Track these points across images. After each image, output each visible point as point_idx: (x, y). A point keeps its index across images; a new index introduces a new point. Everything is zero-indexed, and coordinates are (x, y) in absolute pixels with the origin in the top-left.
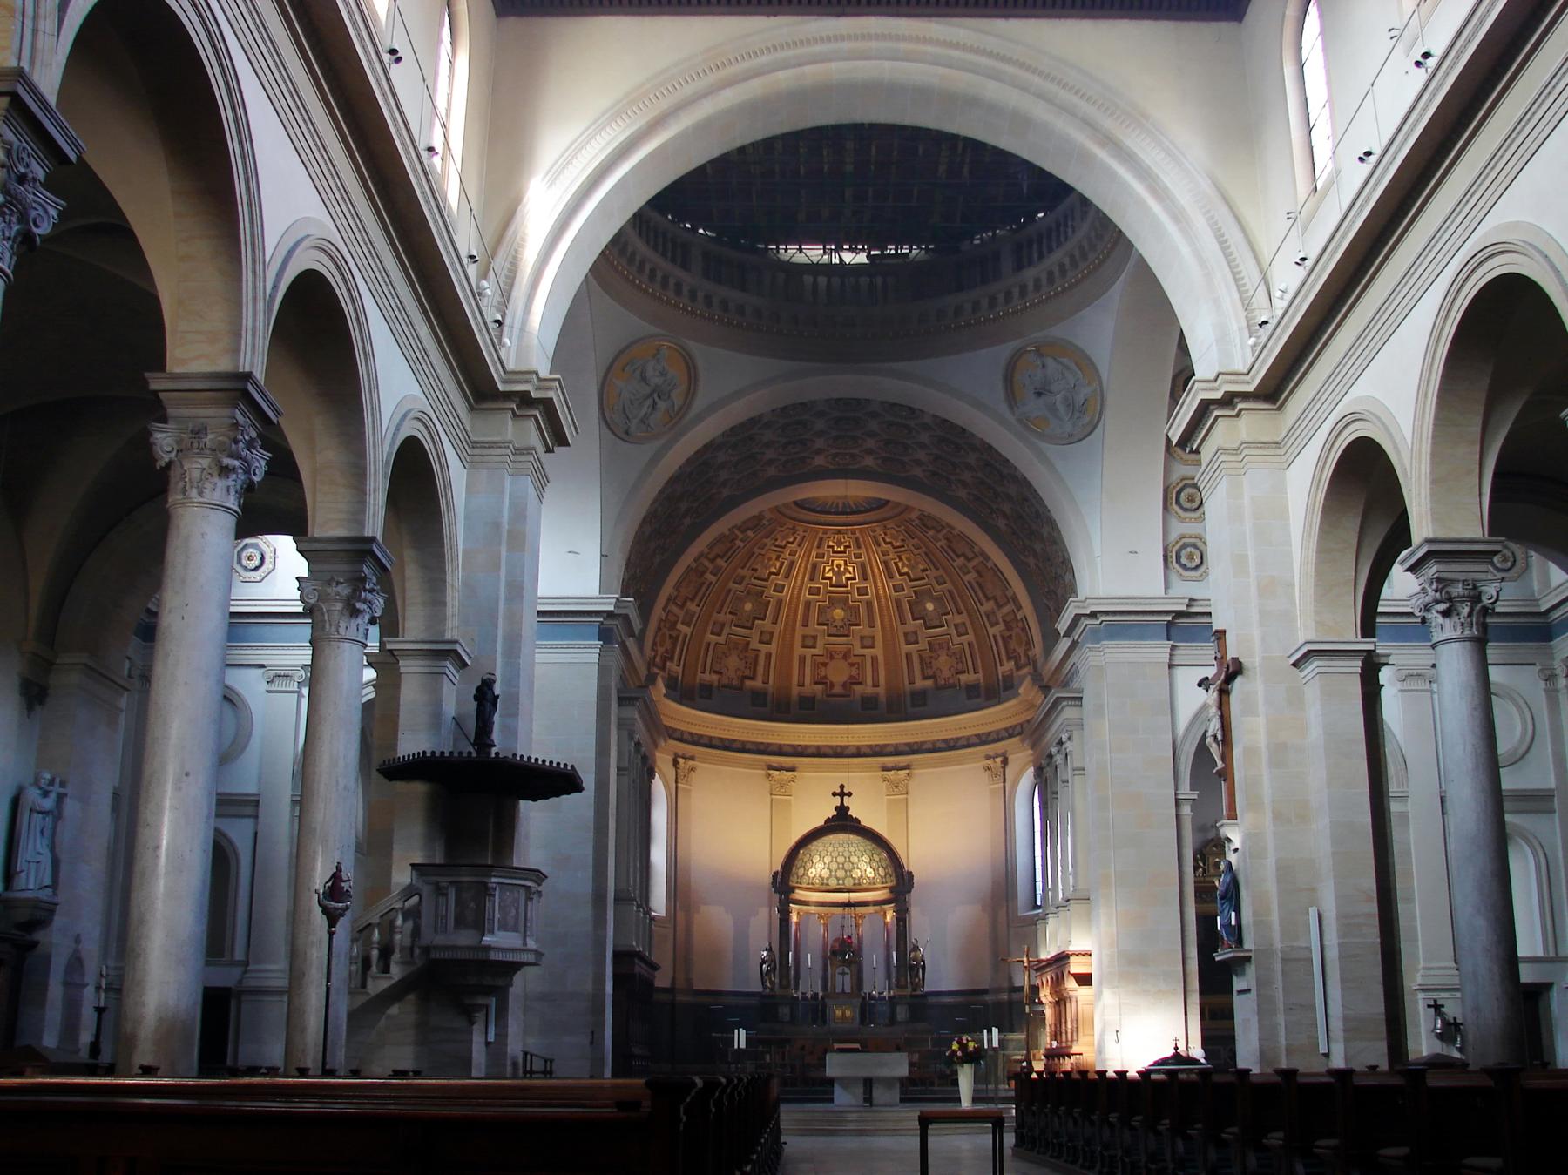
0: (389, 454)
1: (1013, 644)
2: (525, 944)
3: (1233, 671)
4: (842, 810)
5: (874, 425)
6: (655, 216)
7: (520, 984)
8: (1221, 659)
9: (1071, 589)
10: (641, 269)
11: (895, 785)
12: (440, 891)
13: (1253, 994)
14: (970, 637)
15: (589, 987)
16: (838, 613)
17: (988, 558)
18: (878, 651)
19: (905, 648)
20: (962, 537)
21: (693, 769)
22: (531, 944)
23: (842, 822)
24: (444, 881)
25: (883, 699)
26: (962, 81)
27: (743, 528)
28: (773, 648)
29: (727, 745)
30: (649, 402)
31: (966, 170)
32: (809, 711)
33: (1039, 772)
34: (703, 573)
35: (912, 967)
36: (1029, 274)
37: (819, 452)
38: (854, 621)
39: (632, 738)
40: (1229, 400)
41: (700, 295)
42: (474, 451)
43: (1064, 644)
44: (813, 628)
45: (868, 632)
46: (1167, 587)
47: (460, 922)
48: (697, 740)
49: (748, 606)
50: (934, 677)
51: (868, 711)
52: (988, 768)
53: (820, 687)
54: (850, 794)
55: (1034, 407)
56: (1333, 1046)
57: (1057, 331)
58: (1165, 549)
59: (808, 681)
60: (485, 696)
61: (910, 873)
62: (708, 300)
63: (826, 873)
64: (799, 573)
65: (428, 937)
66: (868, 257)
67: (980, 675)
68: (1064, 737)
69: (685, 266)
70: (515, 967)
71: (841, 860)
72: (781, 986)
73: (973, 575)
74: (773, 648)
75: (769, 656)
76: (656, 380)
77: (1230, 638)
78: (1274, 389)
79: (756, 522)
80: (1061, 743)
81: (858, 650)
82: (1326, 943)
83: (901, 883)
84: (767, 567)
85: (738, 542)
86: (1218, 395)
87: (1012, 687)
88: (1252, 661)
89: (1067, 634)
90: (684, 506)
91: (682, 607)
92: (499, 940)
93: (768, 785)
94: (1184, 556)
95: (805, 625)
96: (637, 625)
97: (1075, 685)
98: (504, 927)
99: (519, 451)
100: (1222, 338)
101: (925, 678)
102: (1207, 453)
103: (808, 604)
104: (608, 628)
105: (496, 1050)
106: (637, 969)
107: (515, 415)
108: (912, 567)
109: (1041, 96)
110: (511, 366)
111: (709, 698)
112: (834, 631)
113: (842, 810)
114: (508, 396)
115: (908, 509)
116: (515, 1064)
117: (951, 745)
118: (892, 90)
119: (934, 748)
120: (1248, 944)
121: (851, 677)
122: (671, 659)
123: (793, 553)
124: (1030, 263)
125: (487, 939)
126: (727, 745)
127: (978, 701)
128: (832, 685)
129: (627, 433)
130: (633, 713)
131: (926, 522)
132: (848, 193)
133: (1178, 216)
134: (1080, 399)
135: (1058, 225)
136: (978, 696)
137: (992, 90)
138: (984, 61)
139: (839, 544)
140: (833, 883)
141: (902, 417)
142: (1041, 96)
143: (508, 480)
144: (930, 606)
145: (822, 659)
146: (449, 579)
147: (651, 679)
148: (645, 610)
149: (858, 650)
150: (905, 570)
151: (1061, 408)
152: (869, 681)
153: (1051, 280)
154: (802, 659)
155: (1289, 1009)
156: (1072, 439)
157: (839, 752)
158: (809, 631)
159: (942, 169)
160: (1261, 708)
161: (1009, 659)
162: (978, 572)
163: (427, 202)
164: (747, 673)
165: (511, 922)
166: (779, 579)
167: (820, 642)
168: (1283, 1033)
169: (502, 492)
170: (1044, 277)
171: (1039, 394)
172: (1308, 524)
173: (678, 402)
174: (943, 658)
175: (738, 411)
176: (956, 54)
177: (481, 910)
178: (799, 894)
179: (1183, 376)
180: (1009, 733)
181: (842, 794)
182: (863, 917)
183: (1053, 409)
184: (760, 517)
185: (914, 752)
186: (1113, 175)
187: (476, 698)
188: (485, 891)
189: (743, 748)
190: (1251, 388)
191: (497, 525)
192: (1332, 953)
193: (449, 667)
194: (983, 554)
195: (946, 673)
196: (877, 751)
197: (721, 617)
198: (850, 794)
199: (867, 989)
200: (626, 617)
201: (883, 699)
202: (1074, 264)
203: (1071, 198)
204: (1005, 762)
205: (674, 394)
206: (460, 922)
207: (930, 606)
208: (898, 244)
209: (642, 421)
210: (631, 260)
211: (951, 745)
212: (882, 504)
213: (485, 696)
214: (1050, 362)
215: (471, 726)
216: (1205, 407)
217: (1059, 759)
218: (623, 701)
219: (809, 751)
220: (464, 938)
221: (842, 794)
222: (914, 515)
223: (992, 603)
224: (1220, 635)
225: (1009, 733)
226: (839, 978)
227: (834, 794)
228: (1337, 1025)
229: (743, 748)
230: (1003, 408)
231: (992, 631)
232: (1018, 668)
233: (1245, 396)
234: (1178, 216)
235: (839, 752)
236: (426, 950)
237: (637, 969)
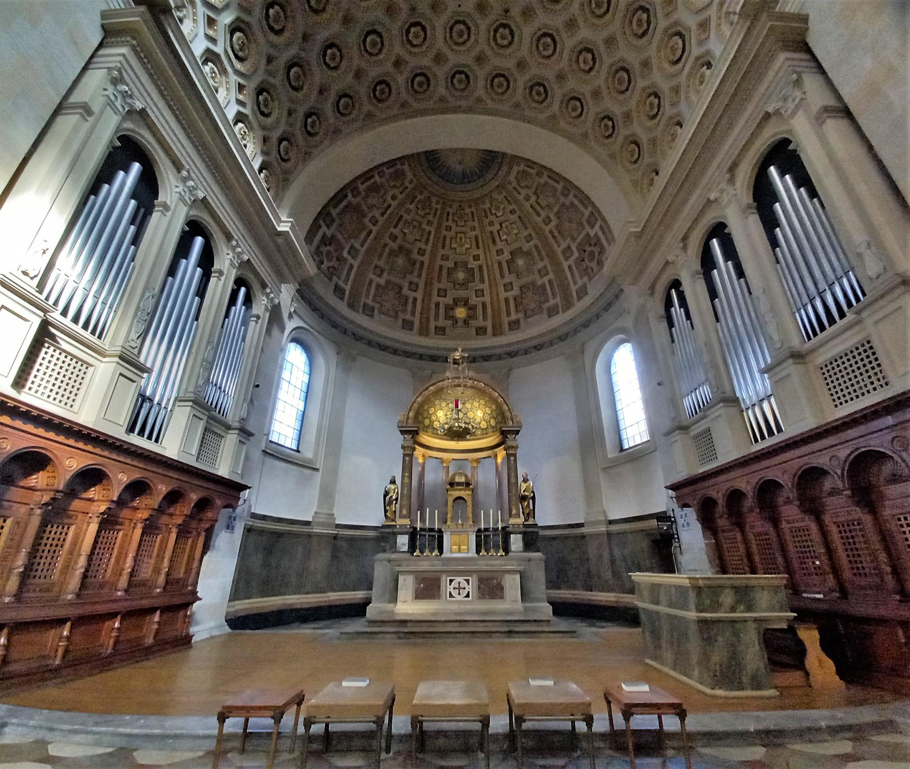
16: (461, 275)
18: (487, 299)
19: (503, 295)
35: (524, 498)
48: (358, 338)
67: (558, 300)
75: (415, 299)
136: (558, 313)
154: (437, 305)
178: (425, 439)
182: (478, 461)
195: (532, 306)
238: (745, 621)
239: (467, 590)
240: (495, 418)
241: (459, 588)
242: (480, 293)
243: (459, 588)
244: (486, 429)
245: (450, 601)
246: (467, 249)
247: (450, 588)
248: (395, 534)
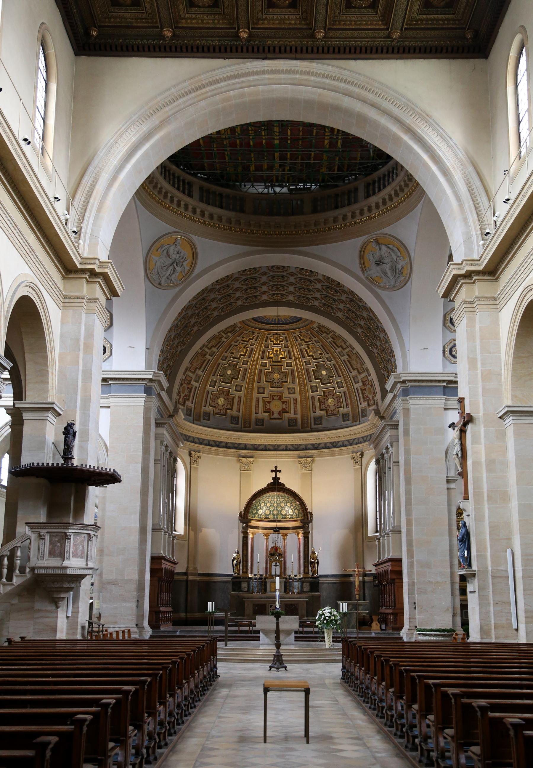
0: (9, 307)
1: (366, 393)
2: (87, 565)
3: (468, 420)
4: (276, 479)
5: (292, 279)
6: (174, 167)
7: (85, 584)
8: (462, 413)
9: (394, 368)
10: (165, 196)
11: (305, 466)
12: (41, 537)
13: (477, 594)
14: (345, 389)
15: (135, 576)
16: (276, 376)
17: (353, 349)
18: (297, 396)
20: (340, 337)
21: (199, 457)
22: (90, 565)
23: (276, 486)
24: (43, 532)
25: (299, 421)
26: (330, 97)
27: (226, 331)
28: (242, 393)
29: (218, 444)
30: (172, 267)
31: (340, 142)
32: (261, 427)
33: (378, 462)
34: (205, 355)
35: (312, 563)
36: (373, 200)
37: (264, 293)
38: (284, 380)
39: (162, 444)
40: (468, 275)
41: (198, 210)
42: (66, 301)
43: (390, 396)
44: (263, 384)
45: (291, 385)
46: (444, 368)
47: (52, 554)
48: (201, 442)
49: (229, 372)
50: (326, 410)
51: (292, 427)
52: (353, 458)
53: (267, 414)
54: (280, 471)
55: (374, 271)
56: (520, 625)
57: (387, 230)
58: (444, 347)
59: (260, 411)
60: (69, 432)
62: (203, 214)
63: (268, 512)
64: (256, 354)
65: (34, 561)
66: (289, 189)
67: (350, 409)
68: (389, 445)
69: (190, 195)
70: (83, 577)
71: (275, 505)
72: (243, 572)
73: (346, 357)
74: (242, 393)
75: (240, 397)
76: (174, 256)
77: (467, 402)
78: (493, 270)
79: (232, 329)
80: (387, 448)
81: (287, 395)
82: (516, 569)
83: (306, 518)
84: (239, 352)
85: (223, 339)
86: (463, 272)
87: (366, 416)
88: (479, 414)
89: (391, 391)
90: (193, 321)
91: (194, 373)
92: (73, 563)
93: (238, 465)
94: (450, 352)
95: (259, 382)
96: (166, 385)
97: (395, 418)
98: (75, 555)
99: (90, 301)
100: (468, 239)
101: (321, 410)
102: (457, 303)
103: (260, 371)
104: (149, 387)
105: (72, 620)
106: (163, 566)
107: (88, 281)
108: (315, 352)
109: (373, 105)
110: (86, 255)
111: (209, 420)
112: (274, 385)
113: (276, 479)
114: (83, 271)
115: (312, 322)
116: (83, 628)
117: (334, 445)
118: (294, 102)
119: (326, 447)
120: (474, 567)
121: (283, 409)
122: (188, 400)
123: (252, 345)
124: (374, 194)
125: (66, 563)
126: (218, 444)
127: (348, 422)
128: (273, 413)
129: (160, 284)
130: (163, 431)
131: (321, 328)
132: (277, 155)
133: (446, 173)
134: (399, 267)
135: (389, 172)
136: (348, 420)
137: (346, 102)
138: (342, 85)
139: (277, 339)
140: (271, 517)
141: (306, 276)
142: (373, 105)
143: (84, 316)
144: (324, 373)
145: (268, 400)
146: (50, 370)
147: (176, 411)
148: (171, 378)
149: (287, 395)
150: (311, 354)
151: (389, 273)
152: (292, 411)
153: (384, 203)
154: (258, 400)
155: (496, 604)
156: (394, 288)
157: (276, 448)
158: (261, 385)
159: (326, 142)
160: (483, 441)
161: (364, 401)
162: (348, 355)
163: (26, 169)
164: (229, 407)
165: (80, 554)
166: (245, 358)
167: (267, 391)
168: (492, 616)
169: (80, 323)
170: (381, 201)
171: (378, 264)
172: (509, 343)
173: (187, 268)
174: (331, 400)
175: (220, 273)
176: (327, 81)
177: (63, 547)
178: (253, 523)
179: (450, 258)
180: (365, 439)
181: (276, 471)
183: (385, 274)
184: (235, 326)
185: (316, 448)
186: (411, 149)
187: (64, 433)
188: (65, 536)
189: (226, 446)
190: (481, 268)
191: (78, 341)
192: (519, 575)
193: (50, 416)
194: (350, 346)
195: (332, 408)
196: (296, 448)
197: (214, 378)
198: (280, 471)
199: (289, 572)
200: (159, 381)
201: (299, 421)
202: (397, 195)
203: (391, 163)
204: (362, 455)
205: (185, 264)
206: (52, 554)
207: (324, 373)
208: (305, 182)
209: (168, 278)
210: (160, 192)
211: (334, 445)
212: (299, 319)
213: (69, 432)
214: (383, 248)
215: (61, 447)
216: (456, 279)
217: (386, 456)
218: (157, 424)
219: (260, 447)
220: (54, 562)
221: (276, 471)
222: (315, 325)
223: (356, 371)
224: (462, 401)
225: (365, 439)
226: (273, 568)
227: (272, 471)
228: (521, 614)
229: (226, 446)
230: (359, 272)
231: (356, 386)
232: (369, 406)
233: (478, 273)
234: (446, 173)
235: (276, 448)
236: (33, 569)
237: (163, 566)
238: (354, 613)
240: (298, 510)
242: (292, 391)
244: (292, 515)
246: (281, 358)
248: (240, 583)
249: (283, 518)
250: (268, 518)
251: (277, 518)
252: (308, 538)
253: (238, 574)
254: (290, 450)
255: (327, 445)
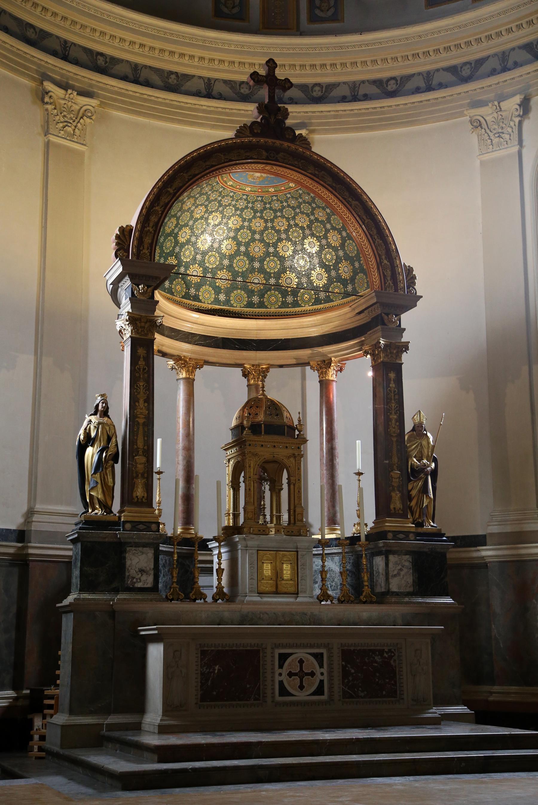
61: (409, 270)
72: (127, 500)
93: (37, 113)
119: (354, 94)
239: (318, 677)
241: (301, 674)
243: (301, 674)
245: (285, 704)
247: (281, 675)
248: (119, 549)
249: (250, 305)
250: (196, 298)
251: (227, 302)
252: (398, 369)
253: (107, 508)
254: (221, 97)
255: (361, 92)
